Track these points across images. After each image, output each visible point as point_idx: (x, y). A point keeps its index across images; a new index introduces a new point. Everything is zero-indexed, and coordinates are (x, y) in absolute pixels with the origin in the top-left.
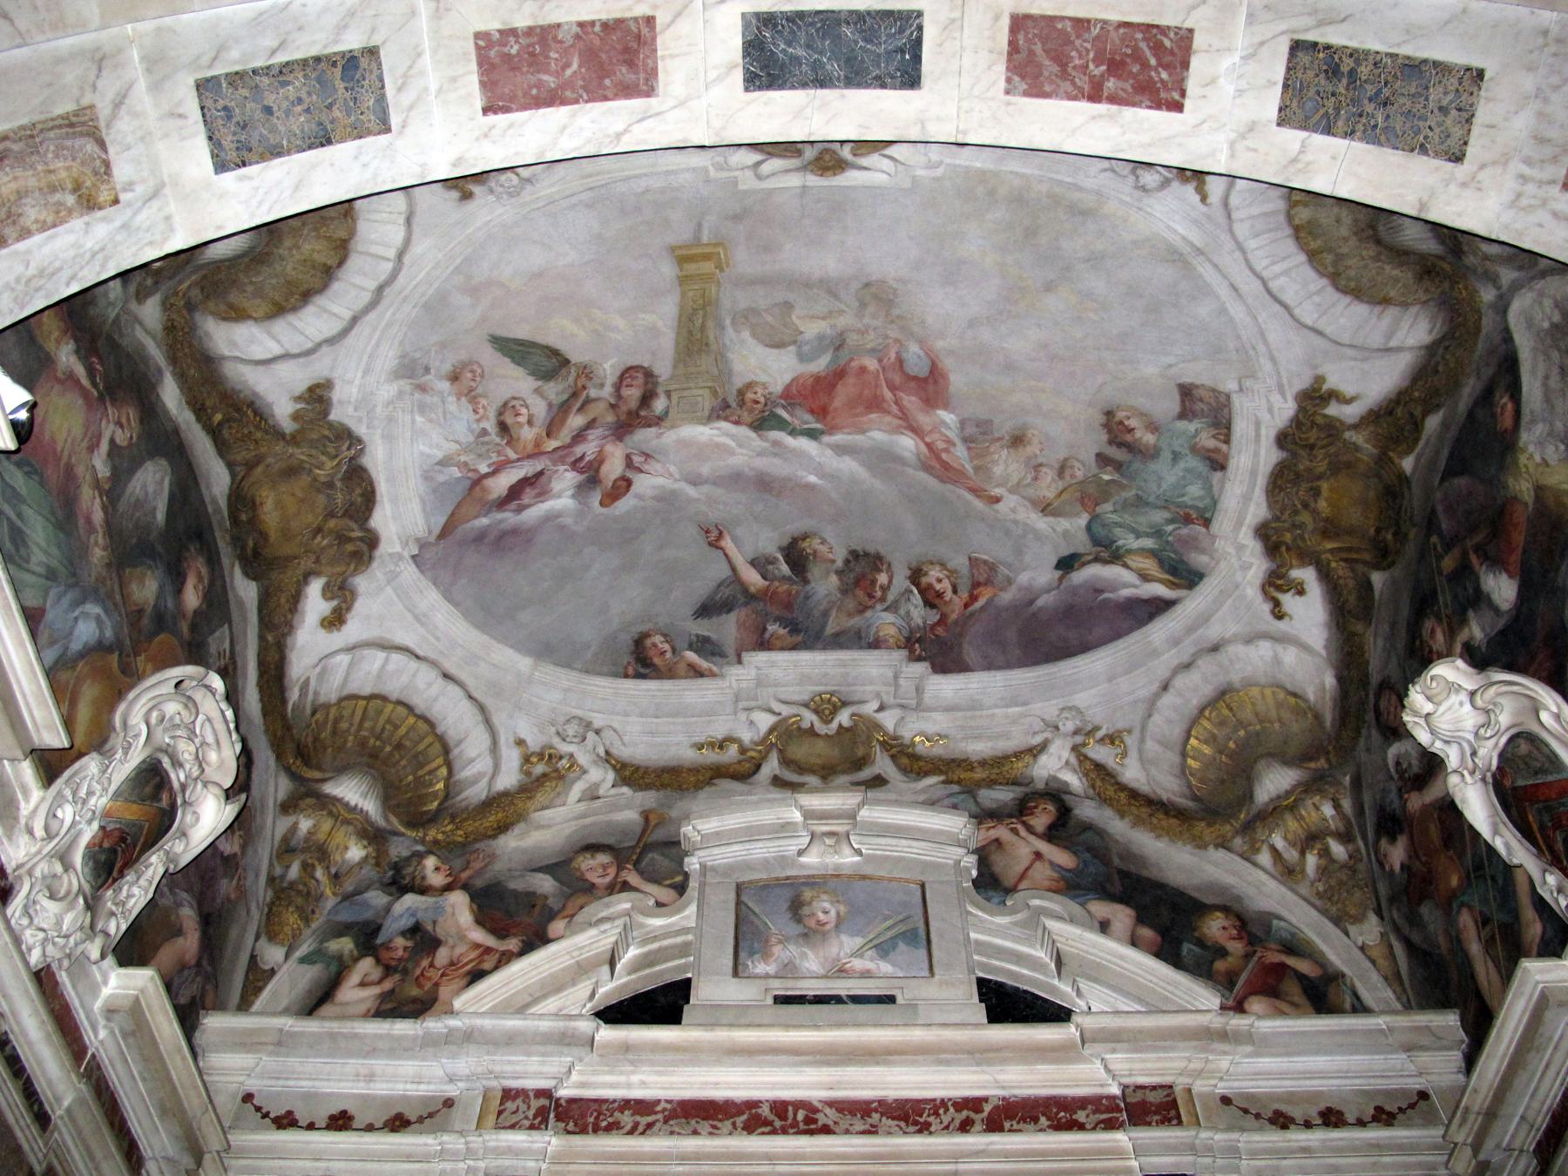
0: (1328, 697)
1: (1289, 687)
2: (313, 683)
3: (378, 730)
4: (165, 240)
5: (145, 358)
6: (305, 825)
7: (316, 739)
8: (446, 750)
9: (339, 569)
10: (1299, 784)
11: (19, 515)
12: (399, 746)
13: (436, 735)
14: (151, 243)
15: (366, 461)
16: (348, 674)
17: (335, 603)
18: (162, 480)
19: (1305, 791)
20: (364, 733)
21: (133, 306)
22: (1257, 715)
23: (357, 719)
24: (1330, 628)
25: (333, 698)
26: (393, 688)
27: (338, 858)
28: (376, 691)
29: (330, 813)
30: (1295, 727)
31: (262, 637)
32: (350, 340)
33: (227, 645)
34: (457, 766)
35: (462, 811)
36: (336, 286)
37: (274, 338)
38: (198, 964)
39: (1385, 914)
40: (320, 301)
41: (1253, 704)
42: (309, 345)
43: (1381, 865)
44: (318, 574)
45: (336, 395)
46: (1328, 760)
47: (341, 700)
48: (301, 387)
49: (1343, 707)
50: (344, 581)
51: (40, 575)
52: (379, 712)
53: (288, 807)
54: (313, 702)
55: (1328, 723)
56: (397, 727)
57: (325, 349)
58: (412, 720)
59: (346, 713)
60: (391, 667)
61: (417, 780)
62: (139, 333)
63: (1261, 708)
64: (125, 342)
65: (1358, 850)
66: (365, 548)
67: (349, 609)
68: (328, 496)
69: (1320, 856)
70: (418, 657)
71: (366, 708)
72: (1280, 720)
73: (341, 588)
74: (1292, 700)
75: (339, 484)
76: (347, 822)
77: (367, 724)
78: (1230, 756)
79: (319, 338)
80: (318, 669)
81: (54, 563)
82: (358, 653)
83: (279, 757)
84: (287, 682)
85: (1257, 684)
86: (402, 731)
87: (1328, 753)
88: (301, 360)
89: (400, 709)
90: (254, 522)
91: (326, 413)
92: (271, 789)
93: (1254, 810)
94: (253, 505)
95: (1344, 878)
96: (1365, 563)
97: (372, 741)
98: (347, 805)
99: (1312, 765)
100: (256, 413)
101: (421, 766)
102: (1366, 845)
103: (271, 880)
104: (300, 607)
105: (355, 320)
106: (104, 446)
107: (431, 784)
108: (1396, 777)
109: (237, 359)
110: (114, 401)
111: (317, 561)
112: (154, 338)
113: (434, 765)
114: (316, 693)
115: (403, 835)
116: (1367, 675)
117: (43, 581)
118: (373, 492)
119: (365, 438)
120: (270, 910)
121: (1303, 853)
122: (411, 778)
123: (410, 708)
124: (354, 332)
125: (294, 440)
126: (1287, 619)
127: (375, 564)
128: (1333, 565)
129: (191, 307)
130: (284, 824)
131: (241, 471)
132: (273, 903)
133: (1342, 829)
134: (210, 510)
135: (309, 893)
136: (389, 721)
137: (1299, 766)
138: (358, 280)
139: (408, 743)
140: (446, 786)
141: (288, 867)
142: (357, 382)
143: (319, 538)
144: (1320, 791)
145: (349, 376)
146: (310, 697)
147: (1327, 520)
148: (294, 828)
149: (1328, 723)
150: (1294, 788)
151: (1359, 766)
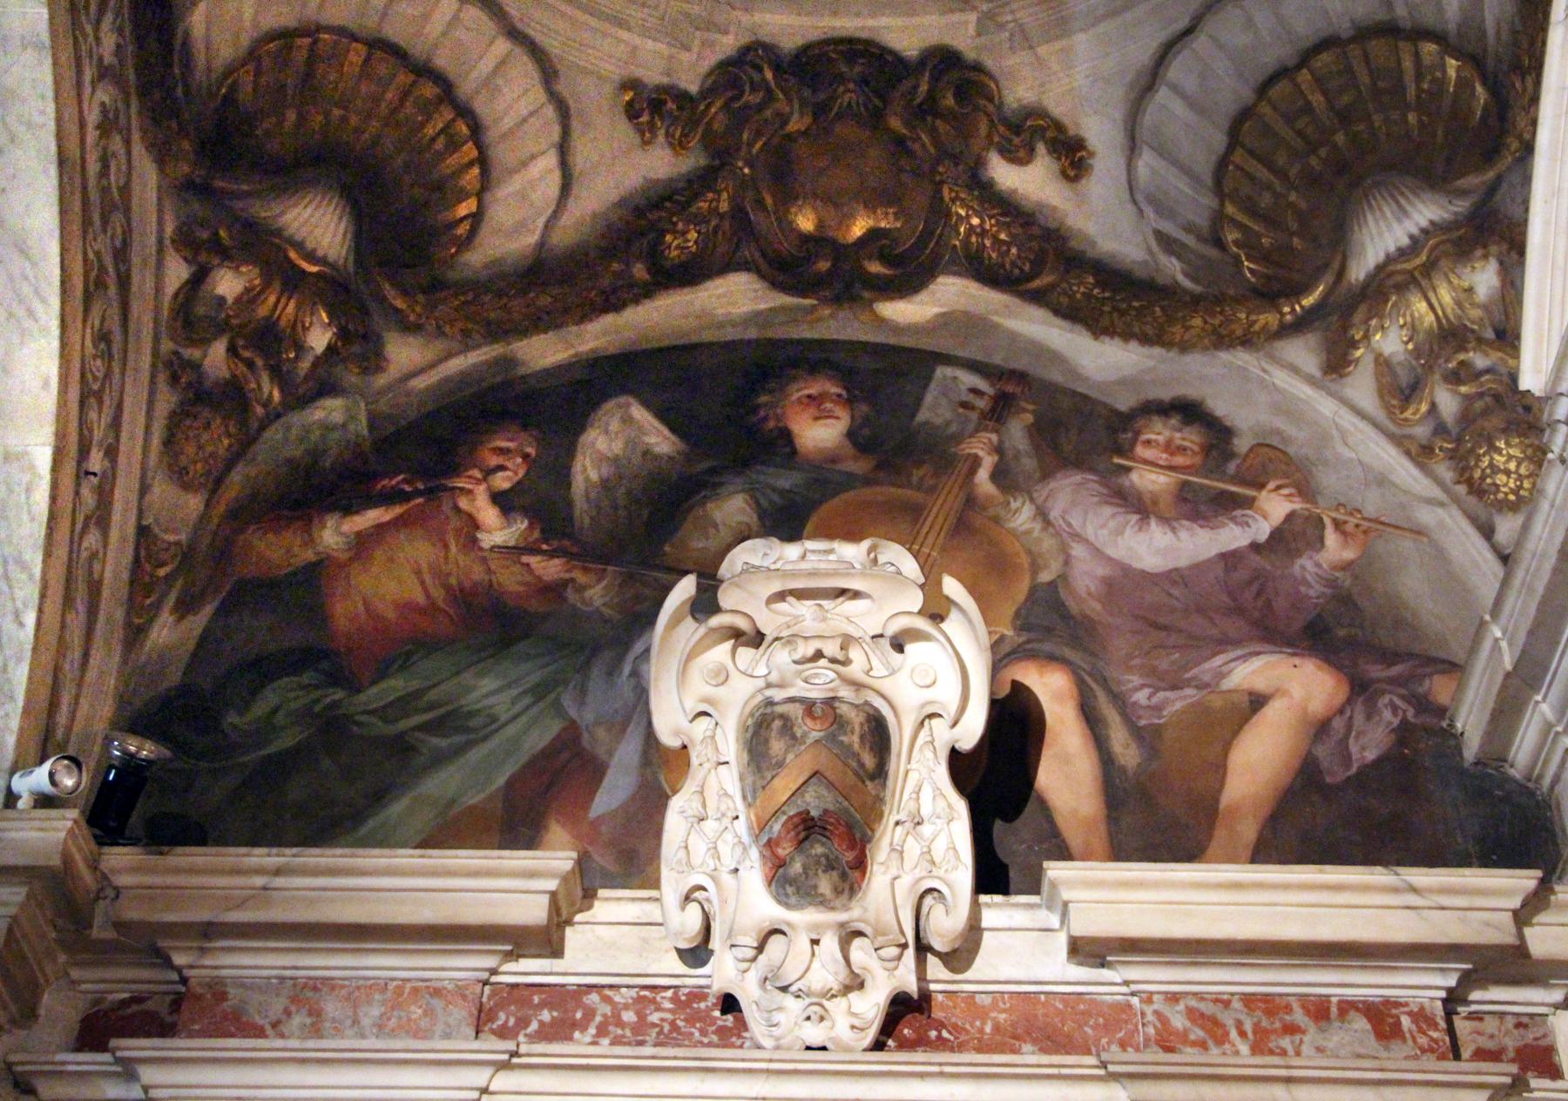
2: (1168, 227)
3: (1298, 143)
4: (32, 467)
5: (464, 378)
6: (1391, 341)
7: (1263, 257)
8: (1389, 30)
9: (983, 128)
11: (432, 707)
12: (1344, 117)
13: (1352, 40)
14: (28, 490)
15: (789, 44)
16: (1175, 162)
17: (1041, 148)
18: (627, 420)
20: (1293, 172)
21: (381, 380)
23: (1263, 173)
25: (1208, 201)
26: (1231, 92)
27: (1476, 313)
28: (1225, 124)
29: (1401, 288)
31: (1037, 298)
32: (552, 45)
33: (968, 379)
34: (1429, 18)
35: (1516, 44)
36: (442, 61)
37: (524, 164)
38: (1360, 688)
40: (465, 88)
42: (550, 112)
44: (980, 162)
45: (653, 76)
47: (1218, 187)
48: (624, 131)
50: (1005, 121)
51: (534, 703)
52: (1267, 130)
53: (1337, 363)
54: (1200, 238)
56: (1308, 109)
57: (561, 87)
58: (1304, 76)
59: (1246, 189)
60: (1191, 84)
61: (1420, 107)
62: (420, 383)
64: (413, 414)
66: (955, 75)
67: (1059, 126)
68: (839, 116)
70: (1188, 32)
71: (1251, 152)
73: (1017, 129)
75: (822, 96)
76: (1429, 269)
77: (1281, 159)
79: (538, 95)
80: (1149, 212)
81: (535, 678)
82: (1144, 133)
83: (1246, 341)
84: (1140, 273)
86: (1317, 99)
88: (575, 124)
89: (1275, 92)
90: (840, 251)
91: (682, 97)
92: (1281, 378)
94: (817, 242)
97: (1314, 161)
98: (1403, 253)
100: (657, 204)
101: (1398, 88)
103: (1421, 455)
104: (1028, 206)
105: (515, 34)
106: (488, 514)
107: (1441, 83)
109: (548, 226)
110: (455, 470)
111: (956, 159)
112: (449, 356)
113: (1408, 64)
114: (1189, 228)
115: (1499, 179)
117: (541, 705)
118: (850, 41)
119: (745, 39)
120: (1469, 482)
122: (1412, 118)
123: (1281, 73)
124: (538, 38)
125: (721, 155)
127: (989, 63)
129: (435, 286)
130: (1362, 386)
131: (748, 252)
132: (1463, 470)
134: (752, 333)
135: (1497, 398)
136: (1289, 119)
138: (436, 26)
139: (1346, 99)
140: (1458, 54)
141: (1433, 407)
142: (637, 41)
143: (916, 147)
145: (621, 51)
146: (1190, 240)
148: (1383, 364)
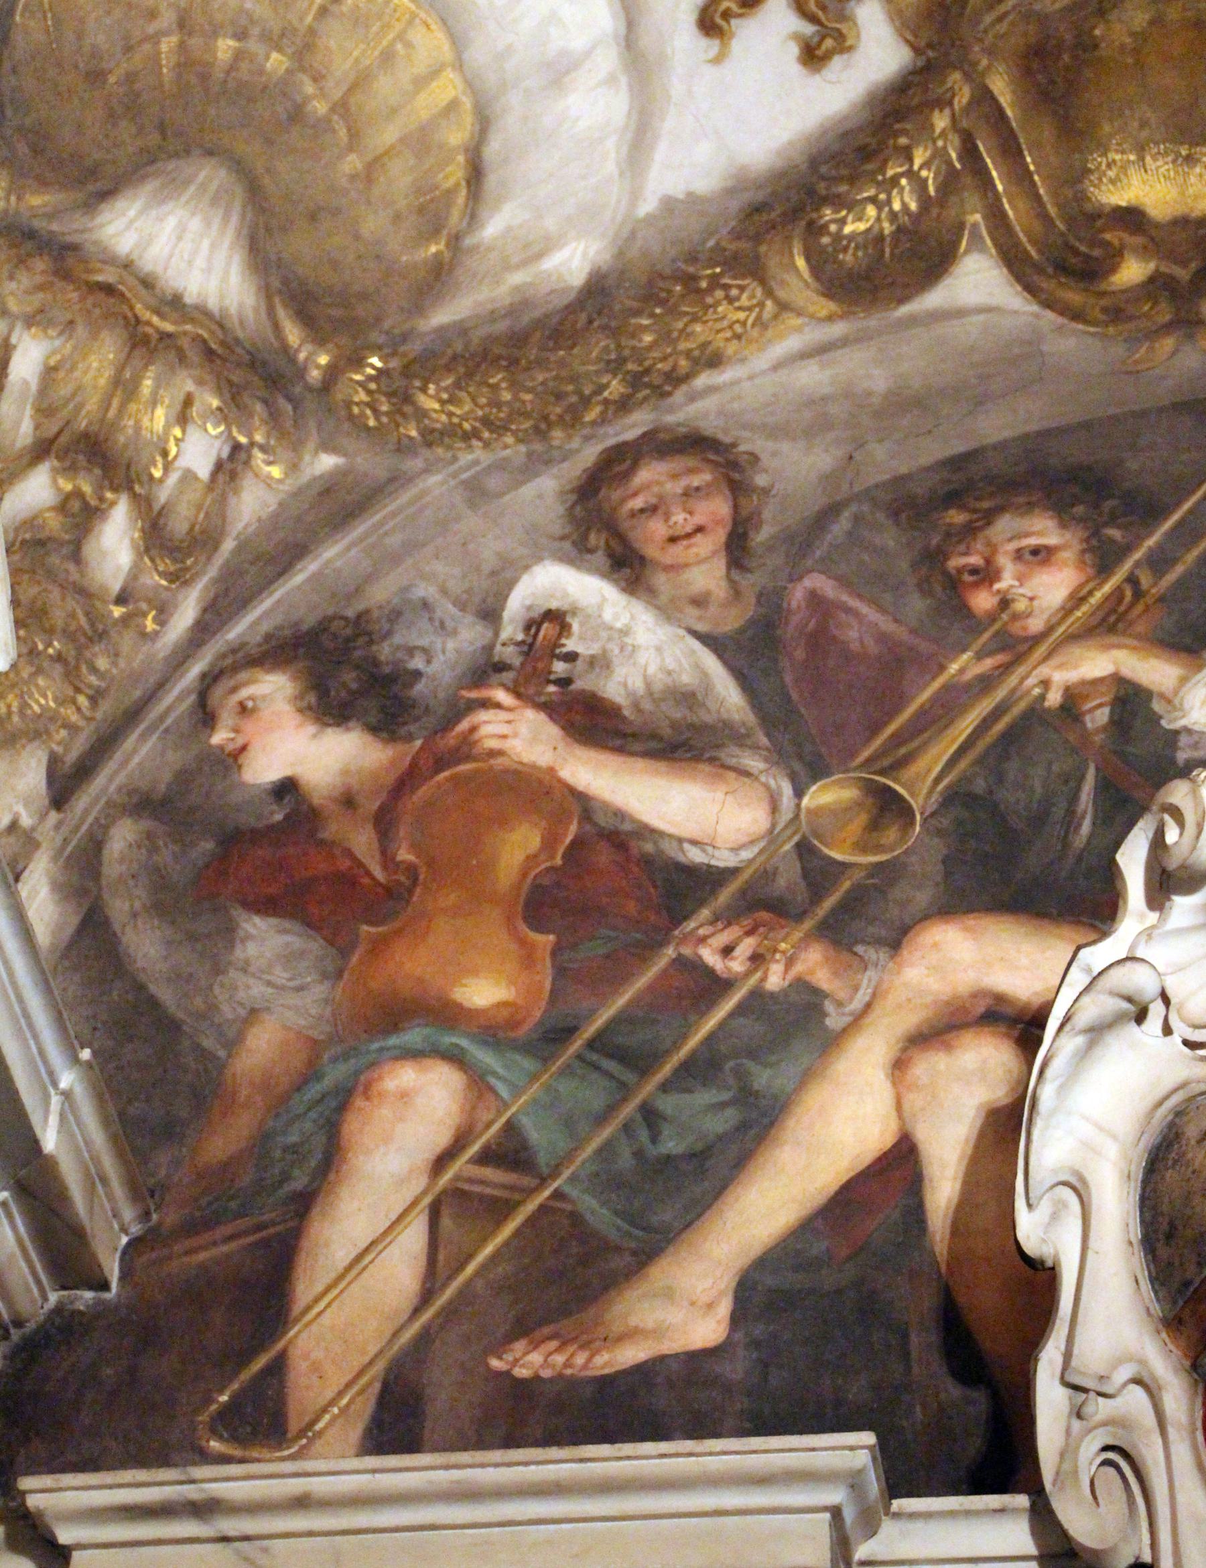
0: (517, 278)
1: (493, 149)
10: (219, 323)
19: (210, 354)
22: (361, 81)
24: (730, 192)
30: (373, 224)
39: (84, 801)
41: (388, 57)
43: (206, 716)
46: (333, 374)
49: (519, 339)
55: (442, 316)
63: (385, 87)
65: (164, 612)
69: (62, 507)
72: (373, 167)
74: (455, 173)
78: (186, 62)
85: (458, 42)
87: (358, 362)
93: (66, 227)
95: (58, 617)
96: (996, 217)
99: (293, 334)
102: (202, 631)
108: (511, 629)
116: (676, 379)
121: (41, 450)
126: (711, 46)
128: (941, 121)
133: (179, 525)
137: (267, 293)
144: (234, 396)
147: (1086, 45)
149: (442, 316)
150: (201, 313)
151: (397, 481)
